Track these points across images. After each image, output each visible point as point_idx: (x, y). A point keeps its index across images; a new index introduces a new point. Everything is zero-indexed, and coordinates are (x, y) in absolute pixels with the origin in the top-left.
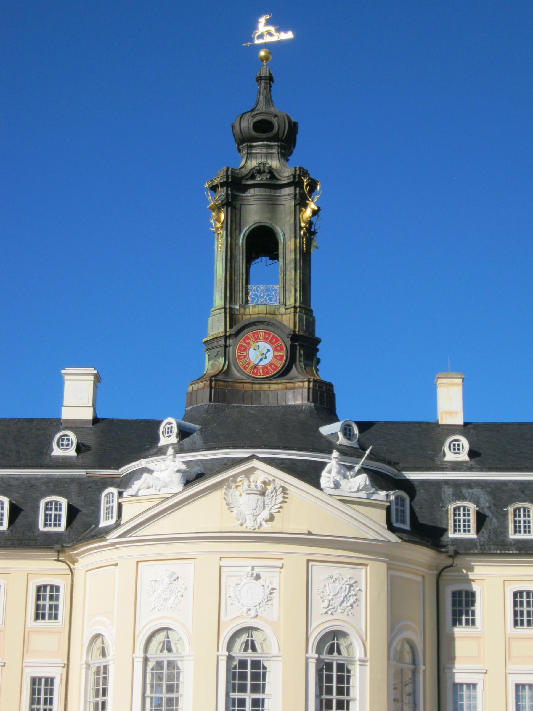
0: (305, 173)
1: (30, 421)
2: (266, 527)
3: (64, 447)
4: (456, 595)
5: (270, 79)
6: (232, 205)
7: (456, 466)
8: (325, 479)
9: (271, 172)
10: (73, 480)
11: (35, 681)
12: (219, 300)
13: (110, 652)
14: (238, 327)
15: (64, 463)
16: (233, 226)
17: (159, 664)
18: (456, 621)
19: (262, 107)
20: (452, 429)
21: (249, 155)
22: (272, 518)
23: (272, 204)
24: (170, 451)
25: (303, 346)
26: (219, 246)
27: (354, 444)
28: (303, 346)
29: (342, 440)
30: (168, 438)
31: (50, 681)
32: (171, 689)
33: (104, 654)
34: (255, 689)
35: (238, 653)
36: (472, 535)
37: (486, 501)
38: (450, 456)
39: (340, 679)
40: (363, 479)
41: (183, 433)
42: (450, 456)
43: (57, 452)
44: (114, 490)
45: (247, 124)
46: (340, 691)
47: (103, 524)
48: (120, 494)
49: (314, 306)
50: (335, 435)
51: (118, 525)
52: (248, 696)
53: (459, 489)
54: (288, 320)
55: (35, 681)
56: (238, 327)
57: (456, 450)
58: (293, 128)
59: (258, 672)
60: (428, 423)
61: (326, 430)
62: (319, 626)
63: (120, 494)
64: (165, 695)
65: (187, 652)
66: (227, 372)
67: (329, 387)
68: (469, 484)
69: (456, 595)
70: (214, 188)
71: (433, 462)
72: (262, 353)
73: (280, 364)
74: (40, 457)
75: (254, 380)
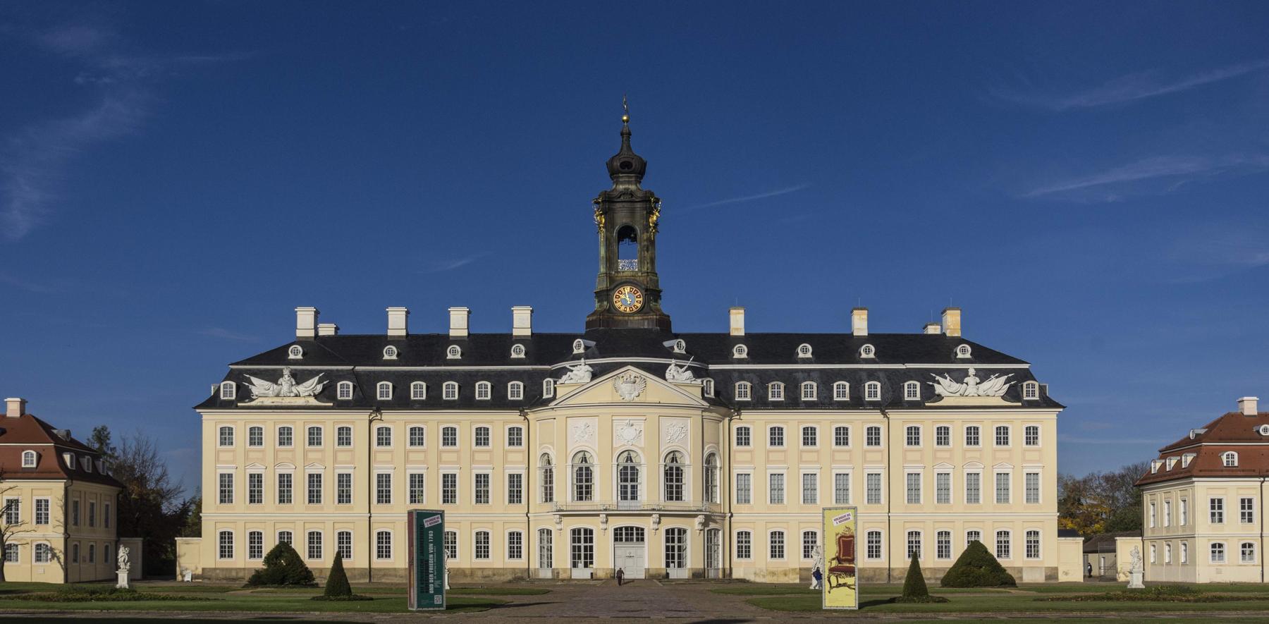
0: (652, 194)
3: (518, 352)
5: (629, 134)
6: (607, 212)
7: (740, 361)
9: (632, 194)
10: (525, 371)
11: (511, 476)
12: (602, 270)
13: (554, 462)
14: (615, 283)
15: (518, 362)
16: (609, 225)
20: (738, 340)
21: (617, 183)
23: (632, 212)
25: (652, 294)
26: (602, 237)
30: (579, 347)
33: (549, 463)
37: (756, 381)
38: (736, 356)
42: (736, 356)
43: (514, 356)
45: (617, 164)
53: (742, 375)
55: (511, 476)
57: (740, 352)
58: (644, 165)
59: (634, 471)
61: (667, 344)
66: (609, 311)
68: (747, 371)
70: (597, 203)
71: (728, 359)
72: (627, 300)
74: (506, 359)
75: (624, 314)
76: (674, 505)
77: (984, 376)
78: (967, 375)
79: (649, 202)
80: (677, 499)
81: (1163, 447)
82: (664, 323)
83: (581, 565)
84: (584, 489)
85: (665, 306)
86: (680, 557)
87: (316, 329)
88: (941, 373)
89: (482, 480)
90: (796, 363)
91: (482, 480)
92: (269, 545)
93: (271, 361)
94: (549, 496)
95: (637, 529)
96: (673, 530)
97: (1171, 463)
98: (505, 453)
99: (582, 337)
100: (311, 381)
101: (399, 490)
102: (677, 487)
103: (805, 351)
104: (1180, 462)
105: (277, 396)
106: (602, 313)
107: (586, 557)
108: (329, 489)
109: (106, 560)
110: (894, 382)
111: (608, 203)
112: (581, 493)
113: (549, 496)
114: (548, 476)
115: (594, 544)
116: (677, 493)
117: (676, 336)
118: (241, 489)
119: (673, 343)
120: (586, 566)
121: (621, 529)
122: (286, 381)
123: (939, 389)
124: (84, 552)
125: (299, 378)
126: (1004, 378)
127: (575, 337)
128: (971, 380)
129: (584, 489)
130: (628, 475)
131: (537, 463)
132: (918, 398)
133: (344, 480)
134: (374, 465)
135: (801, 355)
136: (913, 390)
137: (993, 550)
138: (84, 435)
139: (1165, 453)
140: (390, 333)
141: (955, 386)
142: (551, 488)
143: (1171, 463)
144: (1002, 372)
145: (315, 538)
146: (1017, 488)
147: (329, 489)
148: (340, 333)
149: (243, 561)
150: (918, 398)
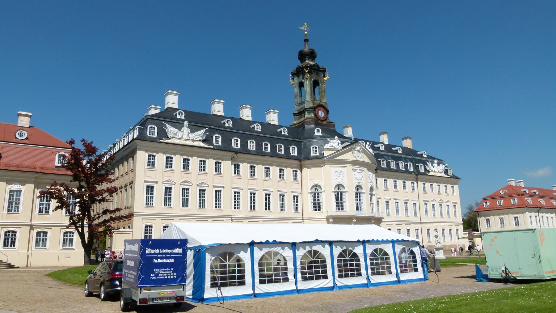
31: (297, 197)
47: (312, 155)
65: (346, 190)
72: (321, 114)
77: (439, 164)
79: (324, 71)
81: (484, 196)
84: (340, 205)
88: (428, 161)
94: (317, 207)
105: (181, 139)
113: (317, 207)
114: (317, 197)
123: (428, 168)
125: (192, 131)
126: (444, 166)
128: (435, 165)
129: (340, 205)
132: (423, 171)
136: (422, 169)
150: (423, 171)
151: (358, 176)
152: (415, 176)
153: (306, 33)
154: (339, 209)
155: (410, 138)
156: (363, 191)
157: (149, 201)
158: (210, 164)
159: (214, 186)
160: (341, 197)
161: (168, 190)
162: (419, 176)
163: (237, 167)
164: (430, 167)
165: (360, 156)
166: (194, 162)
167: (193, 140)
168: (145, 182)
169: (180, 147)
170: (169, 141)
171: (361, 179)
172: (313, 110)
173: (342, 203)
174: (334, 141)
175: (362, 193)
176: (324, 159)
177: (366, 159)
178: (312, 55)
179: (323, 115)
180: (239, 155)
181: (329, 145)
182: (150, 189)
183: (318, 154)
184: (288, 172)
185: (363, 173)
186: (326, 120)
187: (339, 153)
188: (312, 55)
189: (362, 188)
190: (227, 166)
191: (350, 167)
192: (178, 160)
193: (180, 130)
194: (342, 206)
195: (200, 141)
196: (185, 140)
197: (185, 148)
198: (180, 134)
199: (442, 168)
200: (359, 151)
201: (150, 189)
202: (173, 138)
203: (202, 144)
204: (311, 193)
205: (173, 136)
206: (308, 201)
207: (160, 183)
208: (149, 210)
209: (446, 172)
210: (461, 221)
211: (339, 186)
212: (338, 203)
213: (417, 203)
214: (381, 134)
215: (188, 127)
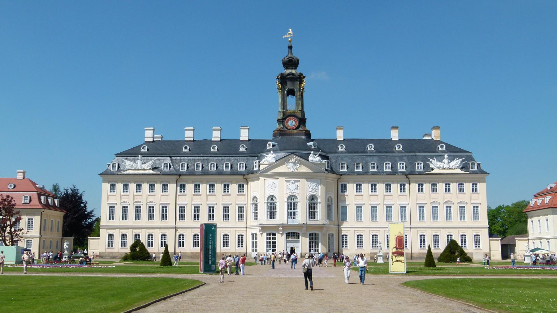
0: (302, 74)
1: (232, 140)
2: (296, 171)
4: (342, 185)
8: (310, 158)
9: (293, 74)
12: (280, 109)
17: (271, 204)
18: (342, 191)
19: (290, 55)
22: (297, 169)
24: (272, 152)
27: (316, 148)
28: (302, 121)
29: (313, 147)
31: (243, 207)
32: (274, 209)
34: (294, 209)
35: (290, 201)
36: (346, 170)
39: (314, 207)
40: (319, 158)
41: (273, 146)
43: (241, 150)
44: (258, 161)
46: (314, 209)
47: (255, 169)
48: (259, 162)
49: (304, 110)
50: (311, 146)
51: (259, 170)
52: (292, 211)
54: (298, 114)
56: (285, 116)
58: (298, 61)
60: (334, 140)
61: (309, 144)
62: (309, 194)
63: (259, 162)
64: (272, 211)
67: (309, 131)
69: (342, 185)
70: (278, 78)
72: (291, 123)
73: (297, 126)
76: (312, 222)
77: (451, 159)
78: (444, 159)
79: (300, 78)
80: (314, 218)
81: (535, 194)
82: (308, 134)
83: (271, 251)
84: (272, 215)
85: (309, 126)
86: (315, 247)
87: (153, 137)
89: (226, 209)
90: (367, 152)
91: (226, 209)
92: (130, 241)
93: (133, 153)
94: (256, 217)
95: (296, 233)
96: (313, 234)
97: (539, 201)
98: (237, 196)
99: (271, 141)
100: (150, 162)
101: (189, 213)
102: (314, 213)
103: (371, 148)
104: (543, 201)
105: (135, 169)
106: (279, 130)
107: (273, 247)
108: (158, 212)
109: (57, 248)
110: (411, 163)
111: (283, 79)
112: (271, 215)
113: (256, 217)
115: (276, 240)
116: (314, 215)
117: (313, 140)
118: (118, 212)
119: (311, 143)
120: (273, 251)
121: (289, 233)
122: (139, 162)
123: (431, 166)
124: (47, 244)
127: (267, 141)
128: (446, 161)
129: (272, 215)
130: (292, 207)
131: (250, 202)
132: (422, 170)
133: (164, 209)
134: (178, 202)
135: (369, 149)
136: (419, 167)
137: (460, 245)
138: (49, 188)
139: (536, 196)
140: (186, 139)
141: (439, 164)
142: (257, 213)
143: (539, 201)
144: (460, 157)
145: (150, 236)
146: (469, 211)
147: (158, 212)
148: (163, 139)
149: (117, 248)
150: (422, 170)
151: (293, 187)
152: (405, 177)
153: (290, 39)
154: (271, 218)
155: (438, 128)
156: (298, 200)
157: (111, 217)
158: (158, 187)
159: (161, 204)
160: (273, 207)
161: (125, 209)
162: (410, 176)
163: (183, 187)
164: (434, 163)
165: (296, 167)
166: (145, 187)
167: (144, 169)
168: (108, 204)
169: (132, 177)
170: (125, 173)
171: (296, 189)
172: (281, 121)
173: (274, 213)
174: (270, 155)
175: (297, 202)
176: (258, 174)
177: (304, 169)
178: (291, 63)
179: (294, 123)
180: (181, 177)
181: (264, 160)
182: (112, 209)
183: (257, 169)
184: (233, 187)
185: (298, 184)
186: (298, 128)
187: (272, 166)
188: (291, 63)
189: (297, 198)
190: (172, 187)
191: (283, 179)
192: (132, 187)
193: (135, 162)
194: (274, 215)
195: (150, 169)
196: (138, 170)
197: (136, 177)
198: (135, 165)
199: (457, 162)
200: (294, 163)
201: (112, 209)
202: (129, 169)
203: (151, 172)
204: (253, 204)
205: (129, 168)
206: (250, 209)
207: (119, 204)
208: (111, 223)
209: (464, 167)
210: (486, 224)
211: (272, 197)
212: (271, 213)
213: (408, 206)
214: (391, 129)
215: (141, 160)
